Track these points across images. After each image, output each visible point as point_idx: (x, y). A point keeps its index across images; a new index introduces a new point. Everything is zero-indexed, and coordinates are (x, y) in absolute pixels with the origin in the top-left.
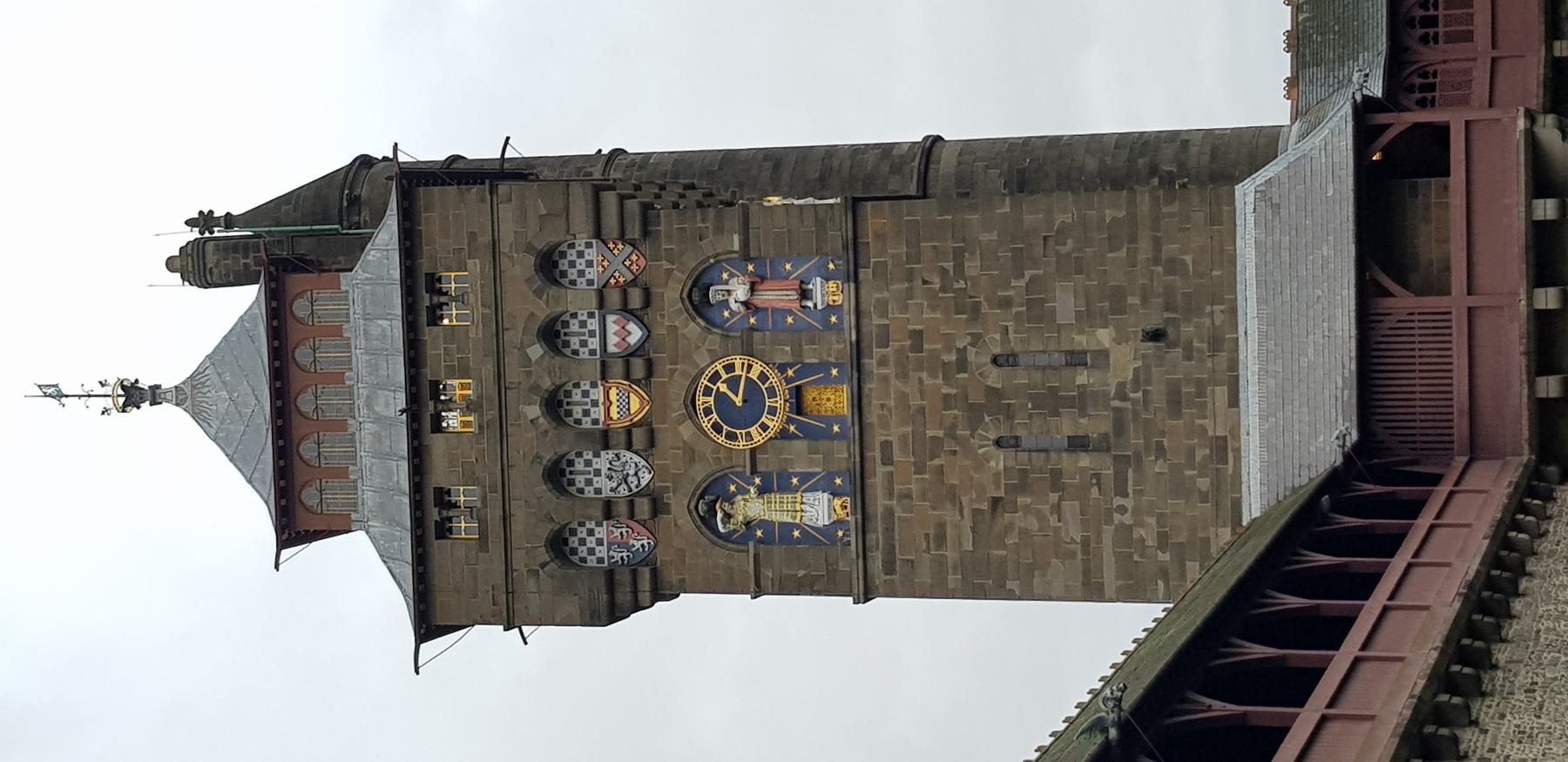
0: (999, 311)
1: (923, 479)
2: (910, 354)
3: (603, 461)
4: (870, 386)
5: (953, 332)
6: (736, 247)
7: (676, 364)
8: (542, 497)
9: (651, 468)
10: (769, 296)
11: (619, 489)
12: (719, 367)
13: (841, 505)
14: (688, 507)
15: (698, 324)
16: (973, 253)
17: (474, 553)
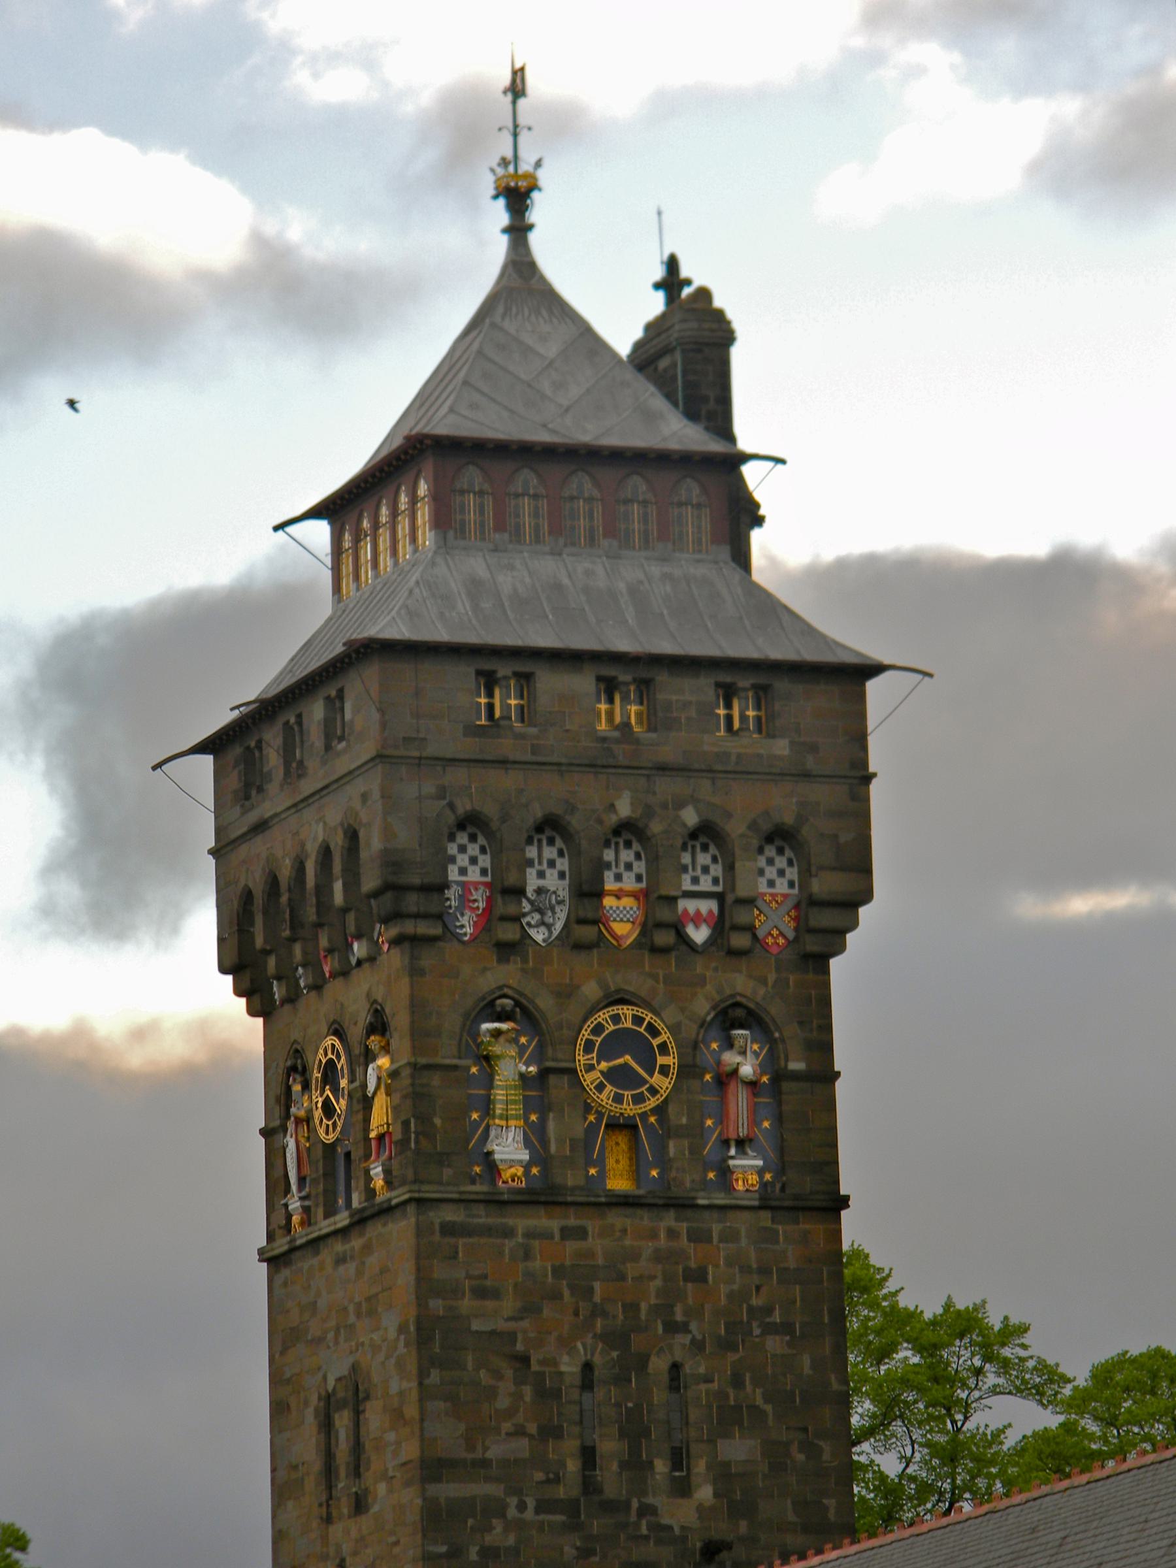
0: (729, 1372)
1: (546, 1276)
2: (680, 1267)
4: (645, 1219)
5: (706, 1320)
7: (665, 983)
10: (740, 1100)
12: (665, 1036)
13: (516, 1175)
15: (708, 1013)
16: (789, 1344)
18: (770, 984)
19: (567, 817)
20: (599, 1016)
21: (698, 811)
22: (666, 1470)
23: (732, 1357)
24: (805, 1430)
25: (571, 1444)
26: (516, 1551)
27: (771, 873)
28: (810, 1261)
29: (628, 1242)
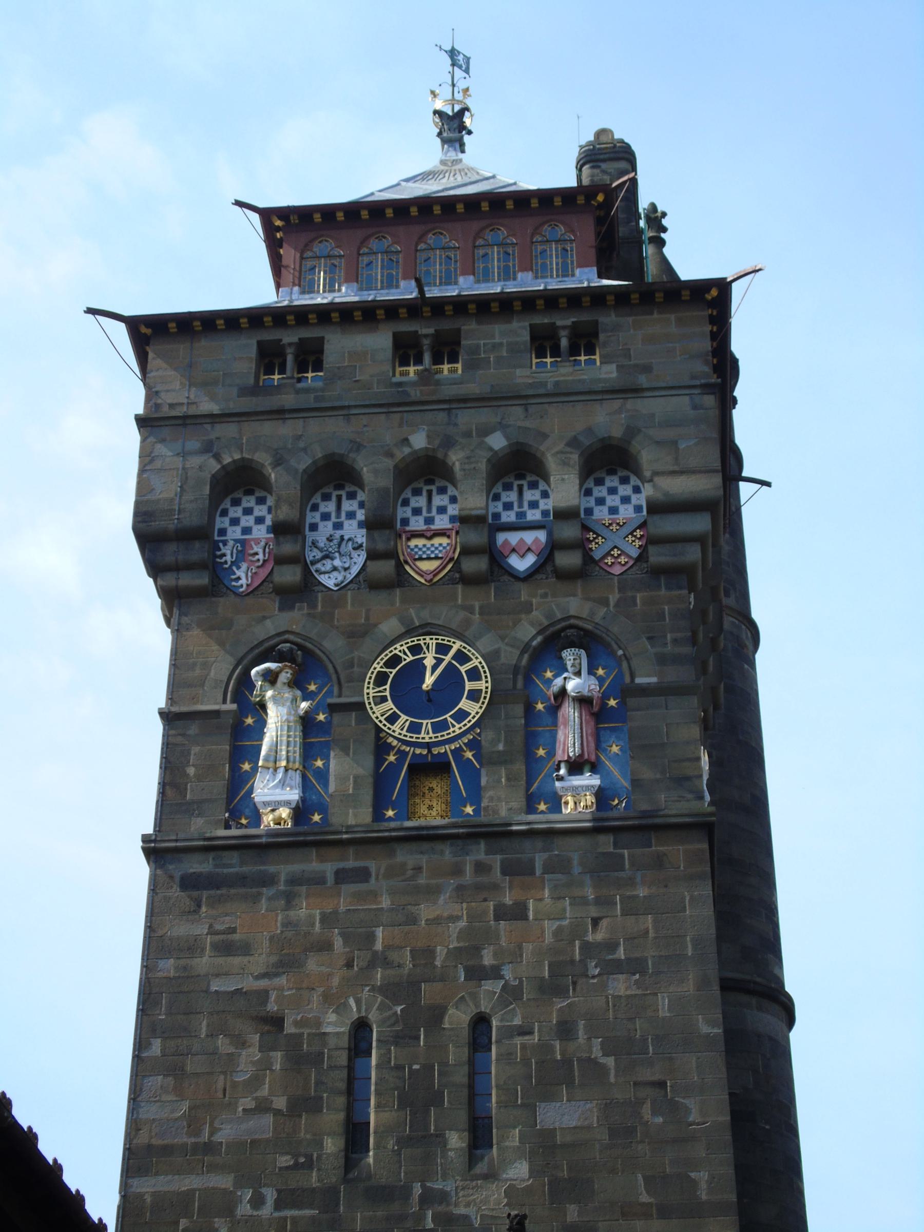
1: (313, 925)
3: (353, 531)
4: (447, 854)
7: (480, 614)
9: (343, 587)
11: (315, 550)
14: (287, 632)
15: (534, 638)
18: (612, 603)
20: (396, 649)
21: (507, 437)
24: (662, 1085)
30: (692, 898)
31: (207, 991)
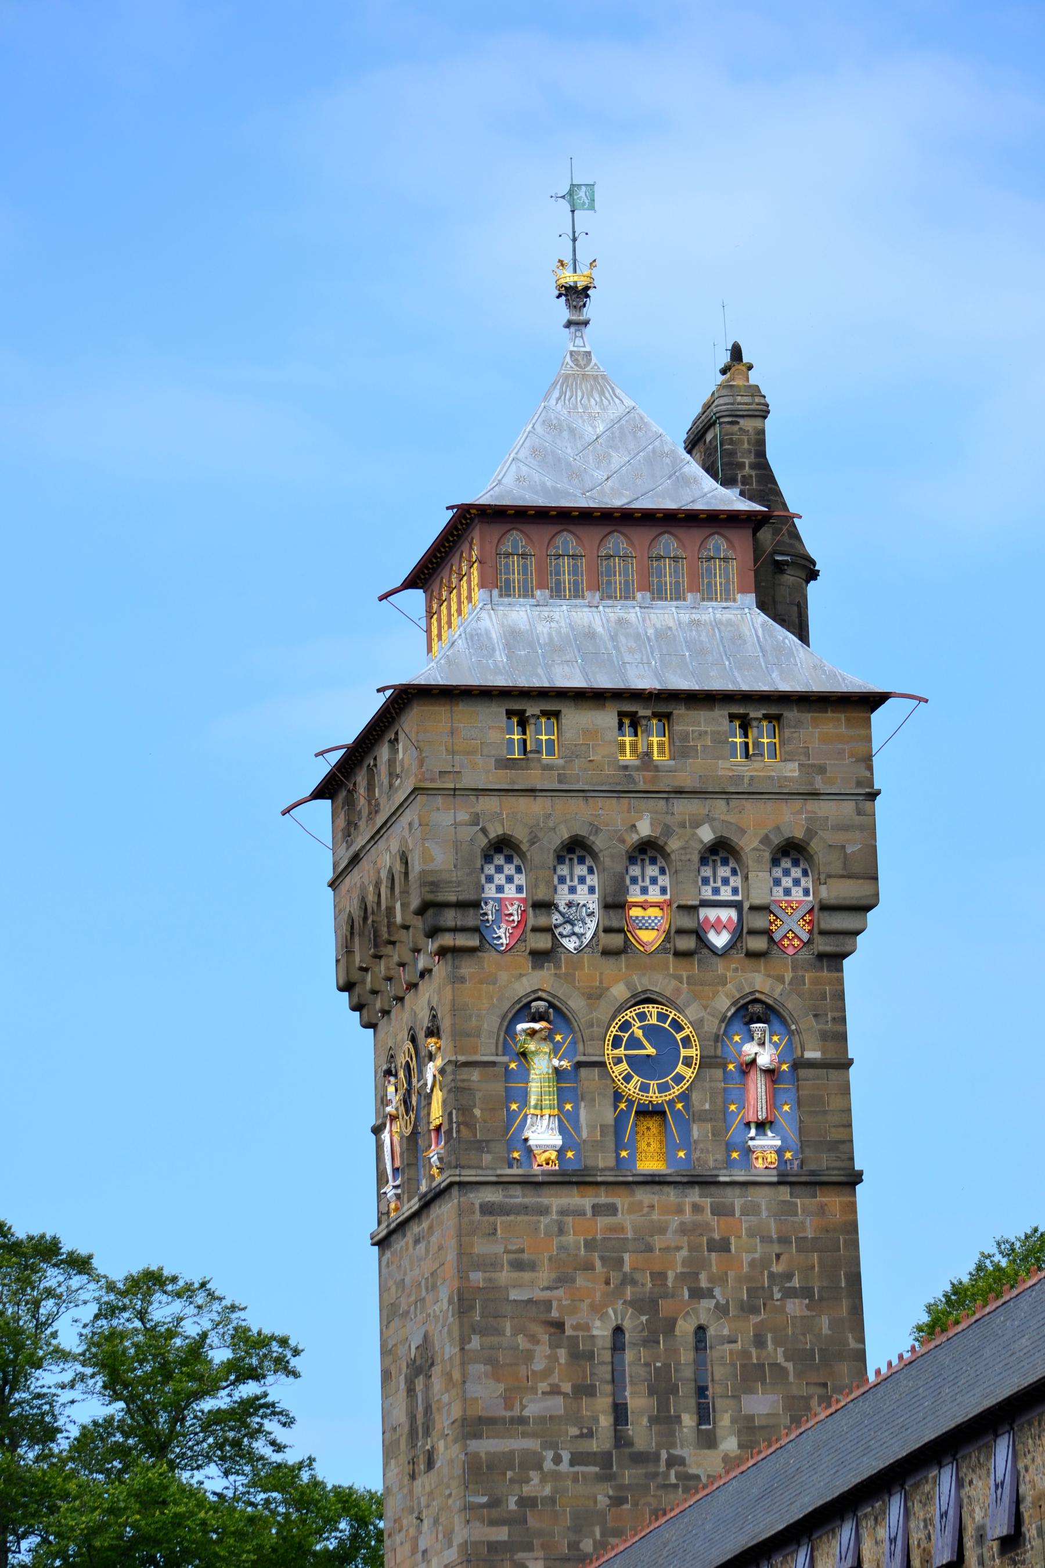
1: (579, 1249)
4: (671, 1195)
6: (809, 1055)
8: (556, 833)
9: (579, 950)
12: (687, 1032)
13: (549, 1159)
15: (728, 1009)
16: (808, 1307)
17: (493, 752)
18: (787, 980)
19: (591, 838)
21: (714, 831)
22: (694, 1424)
23: (755, 1319)
24: (825, 1385)
25: (603, 1402)
26: (552, 1500)
27: (787, 882)
28: (827, 1231)
29: (655, 1217)
30: (845, 1241)
31: (507, 1300)
